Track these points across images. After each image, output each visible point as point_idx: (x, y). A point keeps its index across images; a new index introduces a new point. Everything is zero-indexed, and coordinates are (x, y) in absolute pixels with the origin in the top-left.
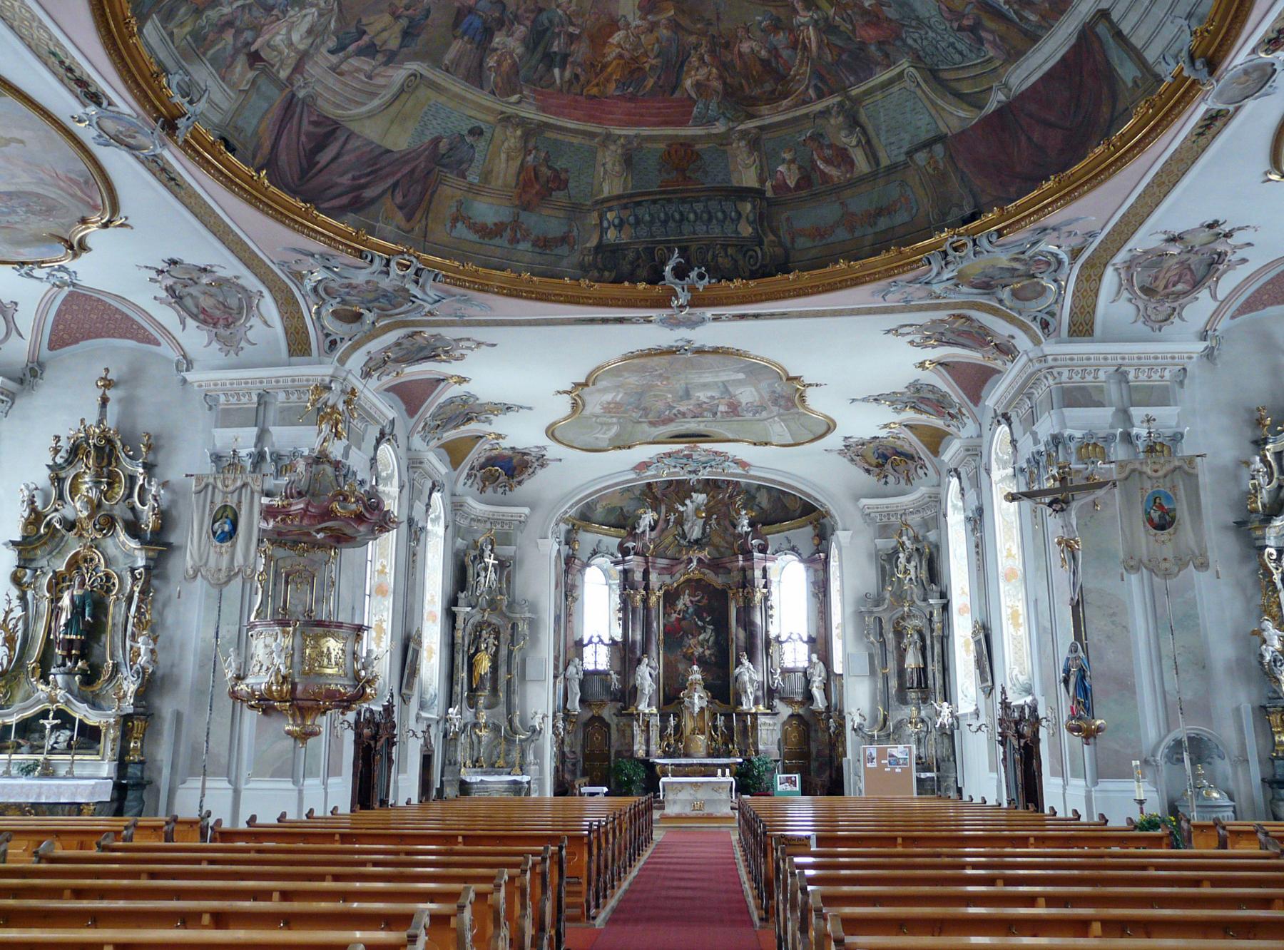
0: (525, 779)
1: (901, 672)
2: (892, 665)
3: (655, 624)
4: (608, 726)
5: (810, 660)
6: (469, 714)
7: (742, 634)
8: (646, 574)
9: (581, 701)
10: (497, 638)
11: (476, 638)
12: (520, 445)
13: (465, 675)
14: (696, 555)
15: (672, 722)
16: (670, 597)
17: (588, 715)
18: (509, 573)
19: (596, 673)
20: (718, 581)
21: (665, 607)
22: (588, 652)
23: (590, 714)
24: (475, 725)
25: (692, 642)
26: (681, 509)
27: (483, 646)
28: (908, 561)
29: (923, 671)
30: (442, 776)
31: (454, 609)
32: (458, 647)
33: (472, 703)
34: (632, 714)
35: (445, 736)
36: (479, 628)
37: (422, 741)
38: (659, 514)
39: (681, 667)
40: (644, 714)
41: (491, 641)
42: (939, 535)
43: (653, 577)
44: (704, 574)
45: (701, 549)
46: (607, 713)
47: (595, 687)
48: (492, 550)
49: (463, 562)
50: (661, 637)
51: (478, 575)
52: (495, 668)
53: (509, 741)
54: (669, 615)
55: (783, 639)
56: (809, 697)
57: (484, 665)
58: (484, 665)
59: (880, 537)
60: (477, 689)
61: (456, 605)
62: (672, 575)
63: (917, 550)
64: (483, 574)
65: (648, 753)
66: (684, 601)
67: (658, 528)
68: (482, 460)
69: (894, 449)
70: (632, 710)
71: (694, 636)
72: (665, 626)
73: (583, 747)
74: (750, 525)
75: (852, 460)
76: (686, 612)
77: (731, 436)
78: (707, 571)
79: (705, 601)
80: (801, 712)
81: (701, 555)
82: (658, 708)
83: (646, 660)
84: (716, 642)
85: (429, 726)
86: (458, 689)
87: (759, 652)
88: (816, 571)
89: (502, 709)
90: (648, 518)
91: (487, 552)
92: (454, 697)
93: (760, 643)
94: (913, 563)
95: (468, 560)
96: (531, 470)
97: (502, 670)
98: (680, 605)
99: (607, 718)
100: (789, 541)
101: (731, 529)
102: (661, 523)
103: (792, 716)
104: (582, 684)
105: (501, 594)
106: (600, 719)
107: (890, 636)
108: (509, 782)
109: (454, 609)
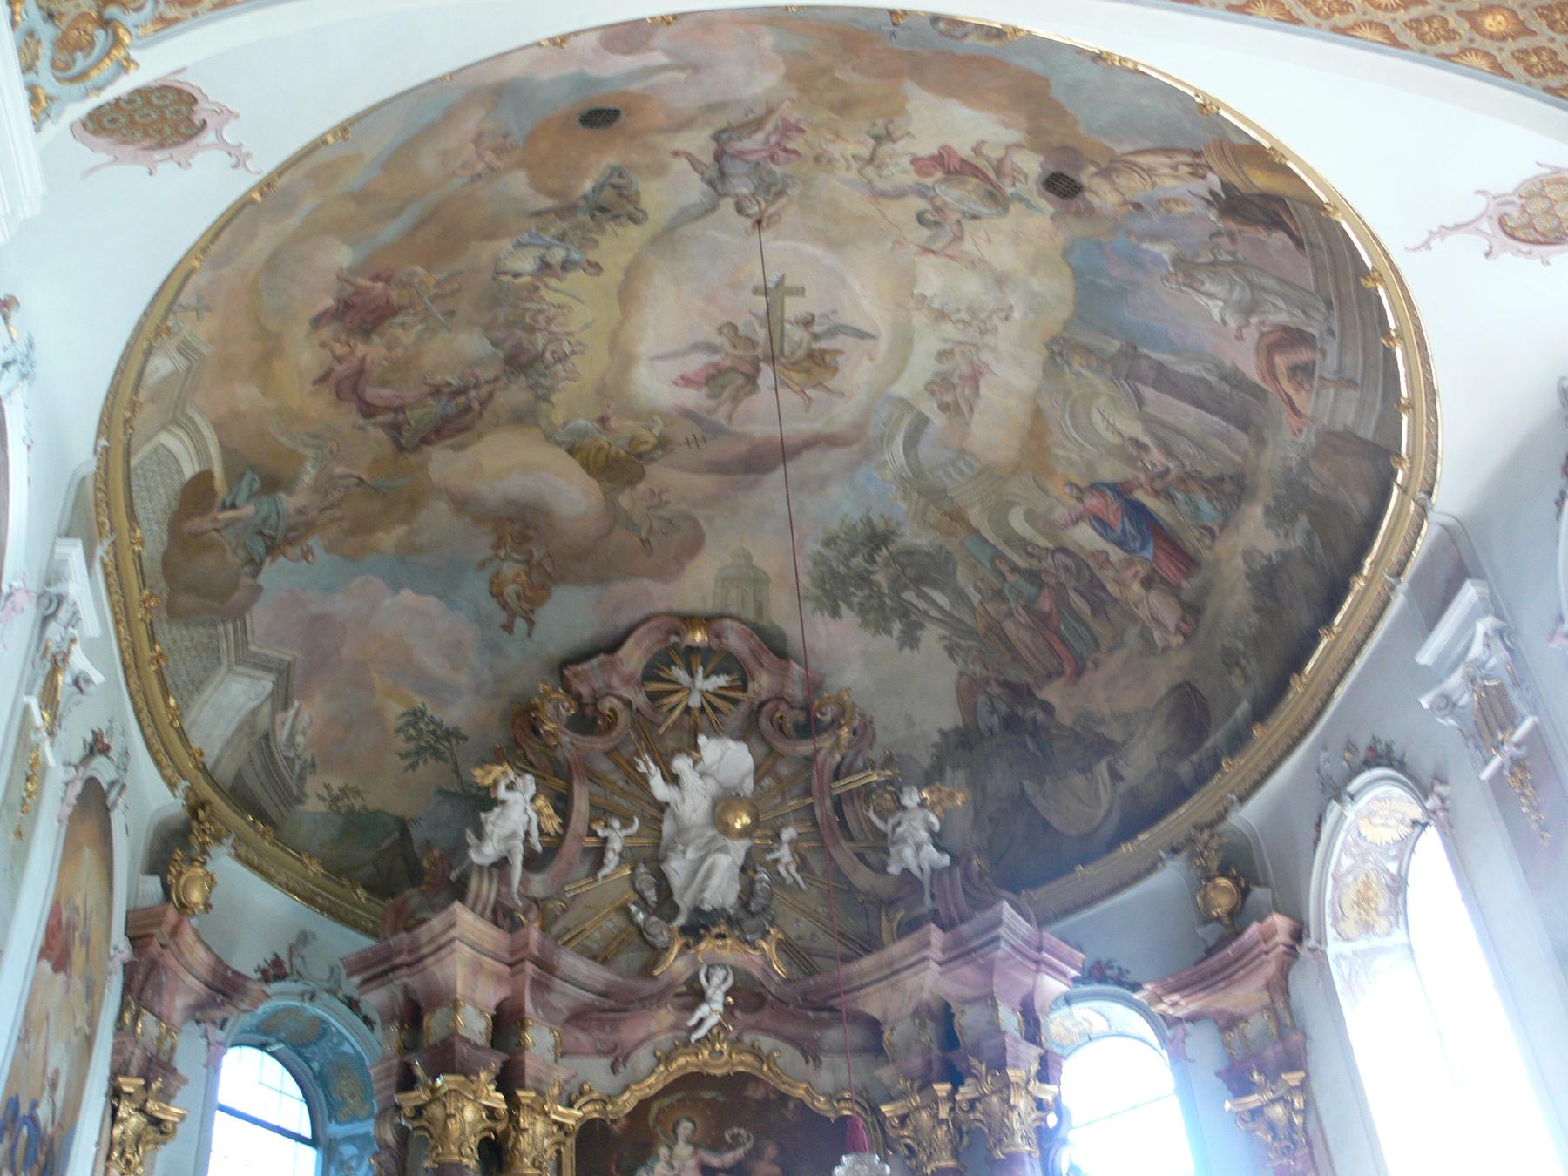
8: (506, 1023)
14: (720, 965)
38: (563, 805)
43: (539, 1040)
44: (755, 1051)
62: (618, 1058)
67: (559, 864)
78: (766, 1043)
102: (570, 847)
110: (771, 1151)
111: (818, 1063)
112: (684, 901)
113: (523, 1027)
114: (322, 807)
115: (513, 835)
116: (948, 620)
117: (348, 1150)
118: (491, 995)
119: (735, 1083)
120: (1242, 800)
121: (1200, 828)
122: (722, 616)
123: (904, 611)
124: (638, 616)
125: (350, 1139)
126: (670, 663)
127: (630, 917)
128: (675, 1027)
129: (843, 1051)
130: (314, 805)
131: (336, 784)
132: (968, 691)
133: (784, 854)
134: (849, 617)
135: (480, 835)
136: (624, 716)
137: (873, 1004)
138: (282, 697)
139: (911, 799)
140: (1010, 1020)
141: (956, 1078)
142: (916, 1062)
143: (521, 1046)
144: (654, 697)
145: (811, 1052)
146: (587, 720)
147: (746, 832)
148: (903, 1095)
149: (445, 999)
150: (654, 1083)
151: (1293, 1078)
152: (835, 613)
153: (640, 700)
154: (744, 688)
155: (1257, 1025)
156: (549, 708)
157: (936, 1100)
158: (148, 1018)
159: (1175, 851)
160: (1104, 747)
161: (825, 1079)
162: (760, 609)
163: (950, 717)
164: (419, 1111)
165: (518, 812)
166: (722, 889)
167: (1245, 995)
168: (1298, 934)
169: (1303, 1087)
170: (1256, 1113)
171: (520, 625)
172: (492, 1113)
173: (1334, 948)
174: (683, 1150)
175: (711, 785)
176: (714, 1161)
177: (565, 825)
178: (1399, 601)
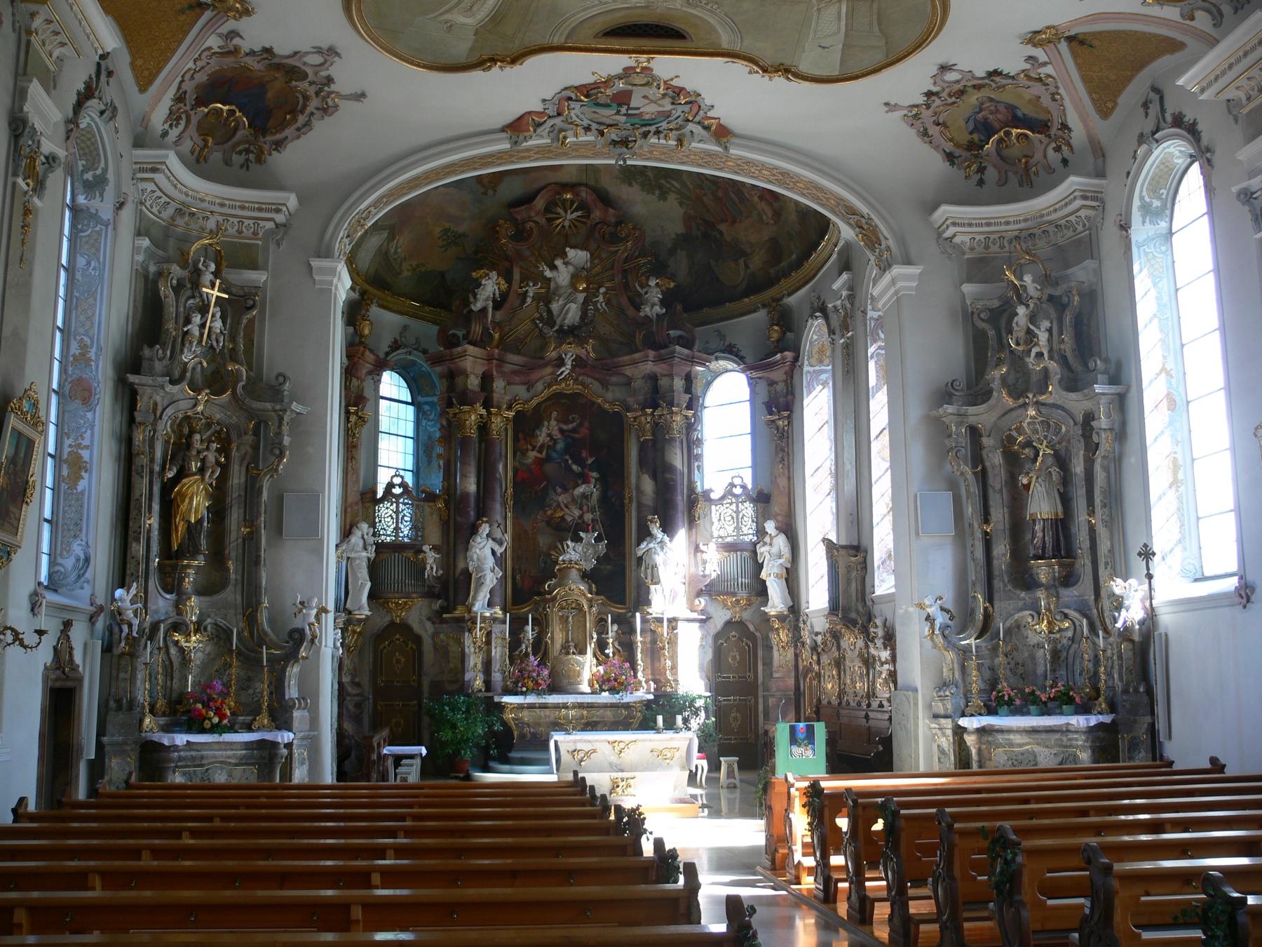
0: (285, 737)
1: (1018, 526)
2: (999, 514)
3: (501, 467)
4: (418, 639)
5: (761, 532)
6: (162, 603)
7: (648, 485)
8: (486, 379)
9: (371, 596)
10: (224, 450)
11: (180, 449)
12: (282, 48)
13: (153, 521)
14: (570, 352)
15: (530, 632)
16: (525, 424)
17: (383, 621)
18: (251, 321)
19: (397, 547)
20: (608, 398)
21: (516, 439)
22: (385, 512)
23: (387, 619)
24: (176, 627)
25: (563, 499)
26: (548, 274)
27: (194, 466)
28: (1033, 318)
29: (1062, 525)
30: (101, 733)
31: (132, 378)
32: (143, 460)
33: (171, 582)
34: (460, 620)
35: (107, 649)
36: (184, 432)
37: (44, 655)
38: (509, 280)
39: (543, 541)
40: (484, 619)
41: (211, 457)
42: (1098, 272)
43: (499, 385)
44: (582, 384)
45: (581, 342)
46: (417, 614)
47: (396, 571)
48: (217, 274)
49: (156, 292)
50: (510, 491)
51: (188, 321)
52: (218, 510)
53: (250, 658)
54: (524, 453)
55: (714, 496)
56: (761, 591)
57: (196, 502)
58: (196, 502)
59: (969, 280)
60: (180, 554)
61: (137, 370)
62: (530, 386)
63: (1051, 299)
64: (197, 319)
65: (488, 684)
66: (549, 430)
67: (507, 306)
68: (202, 78)
69: (1011, 108)
70: (459, 611)
71: (565, 490)
72: (515, 471)
73: (374, 675)
74: (663, 303)
75: (925, 134)
76: (551, 448)
77: (725, 42)
79: (584, 431)
80: (746, 615)
81: (582, 352)
82: (504, 610)
83: (485, 529)
84: (604, 499)
85: (67, 624)
86: (138, 549)
87: (680, 515)
88: (772, 383)
89: (231, 595)
90: (490, 286)
91: (208, 277)
92: (130, 568)
93: (681, 501)
94: (1046, 324)
95: (165, 290)
96: (302, 119)
97: (235, 516)
98: (542, 437)
99: (416, 628)
100: (722, 337)
101: (631, 312)
102: (512, 296)
103: (728, 623)
104: (373, 568)
105: (234, 359)
106: (405, 628)
107: (995, 459)
108: (248, 745)
109: (132, 378)
110: (586, 424)
111: (607, 390)
112: (558, 322)
113: (493, 381)
114: (409, 274)
115: (487, 300)
116: (679, 192)
117: (426, 408)
118: (480, 370)
119: (575, 396)
120: (790, 295)
121: (774, 300)
122: (580, 184)
123: (661, 187)
124: (543, 183)
125: (426, 403)
126: (557, 205)
127: (537, 325)
128: (553, 373)
129: (616, 384)
130: (406, 274)
131: (414, 264)
132: (687, 219)
133: (601, 298)
134: (636, 188)
135: (475, 295)
136: (535, 231)
137: (629, 371)
138: (391, 238)
139: (652, 283)
140: (679, 384)
141: (655, 406)
142: (641, 398)
143: (492, 391)
144: (550, 220)
145: (605, 384)
146: (521, 235)
147: (584, 290)
148: (635, 410)
149: (464, 373)
150: (546, 394)
151: (786, 414)
152: (630, 185)
153: (543, 221)
154: (588, 217)
155: (780, 387)
156: (503, 231)
157: (646, 414)
158: (354, 380)
159: (764, 306)
160: (743, 254)
161: (610, 396)
162: (597, 181)
163: (680, 229)
164: (455, 414)
165: (490, 286)
166: (572, 314)
167: (778, 375)
168: (796, 359)
169: (789, 417)
170: (773, 421)
171: (490, 192)
172: (481, 416)
173: (806, 369)
174: (553, 423)
175: (571, 268)
176: (565, 427)
177: (510, 287)
178: (835, 256)
